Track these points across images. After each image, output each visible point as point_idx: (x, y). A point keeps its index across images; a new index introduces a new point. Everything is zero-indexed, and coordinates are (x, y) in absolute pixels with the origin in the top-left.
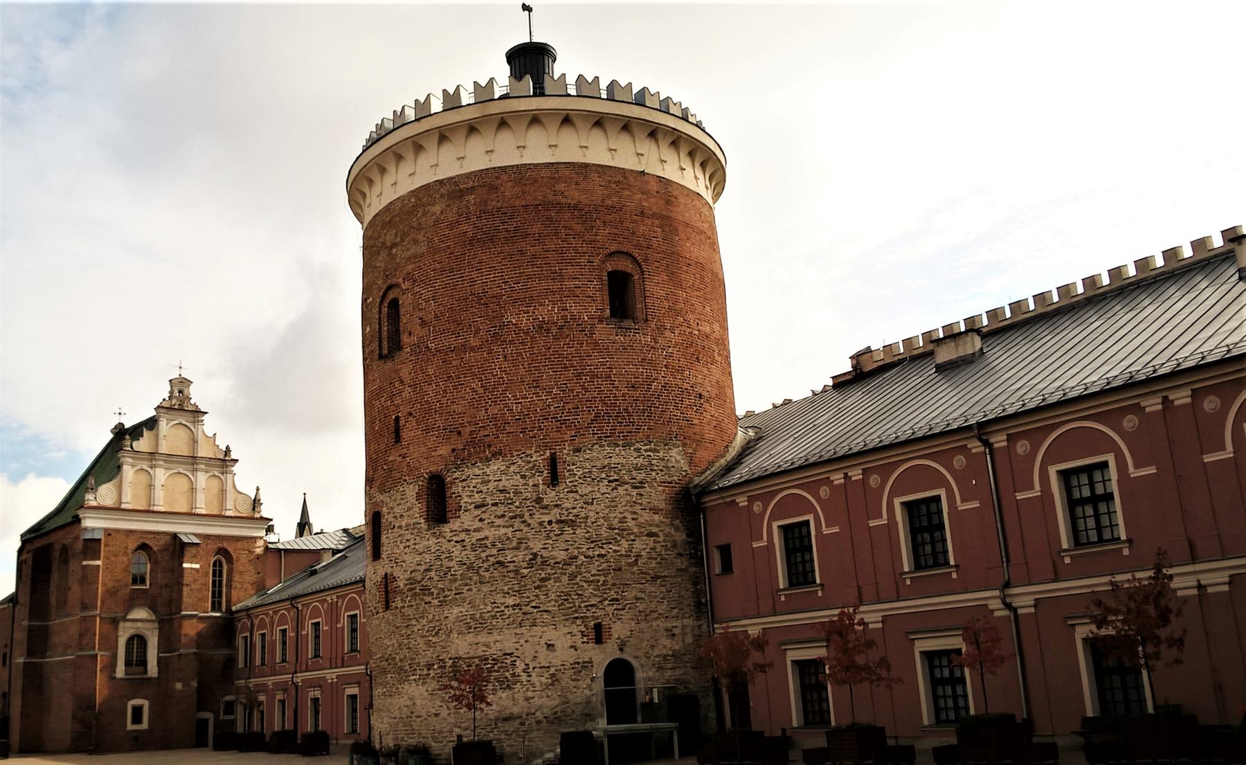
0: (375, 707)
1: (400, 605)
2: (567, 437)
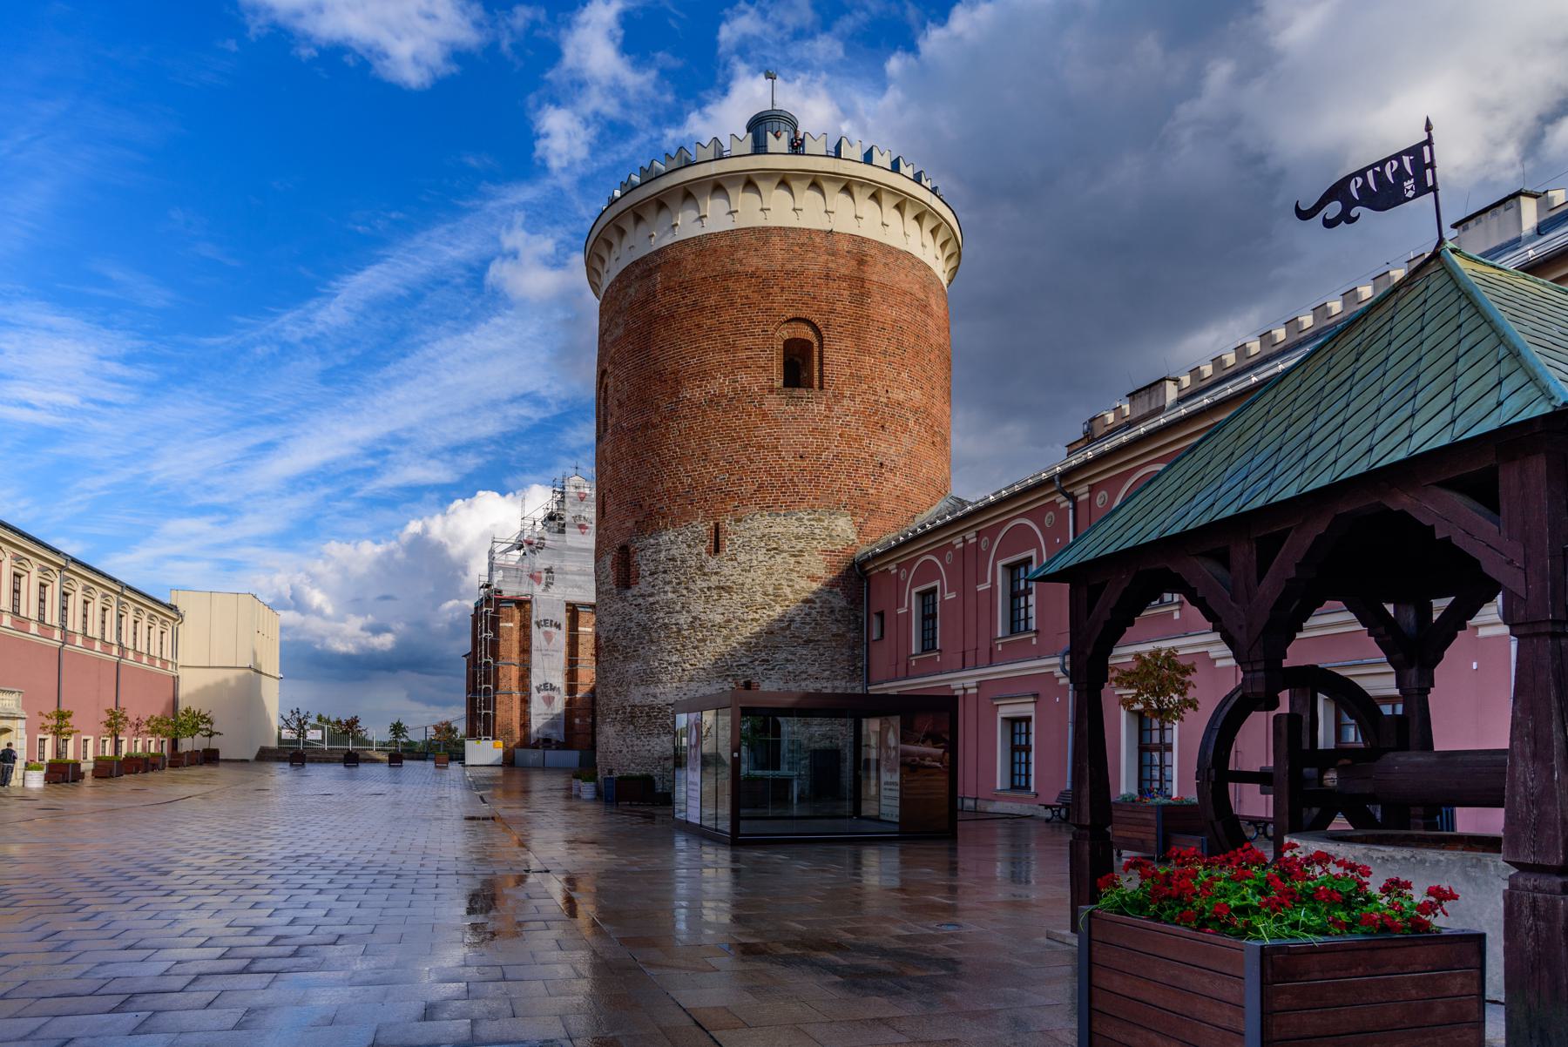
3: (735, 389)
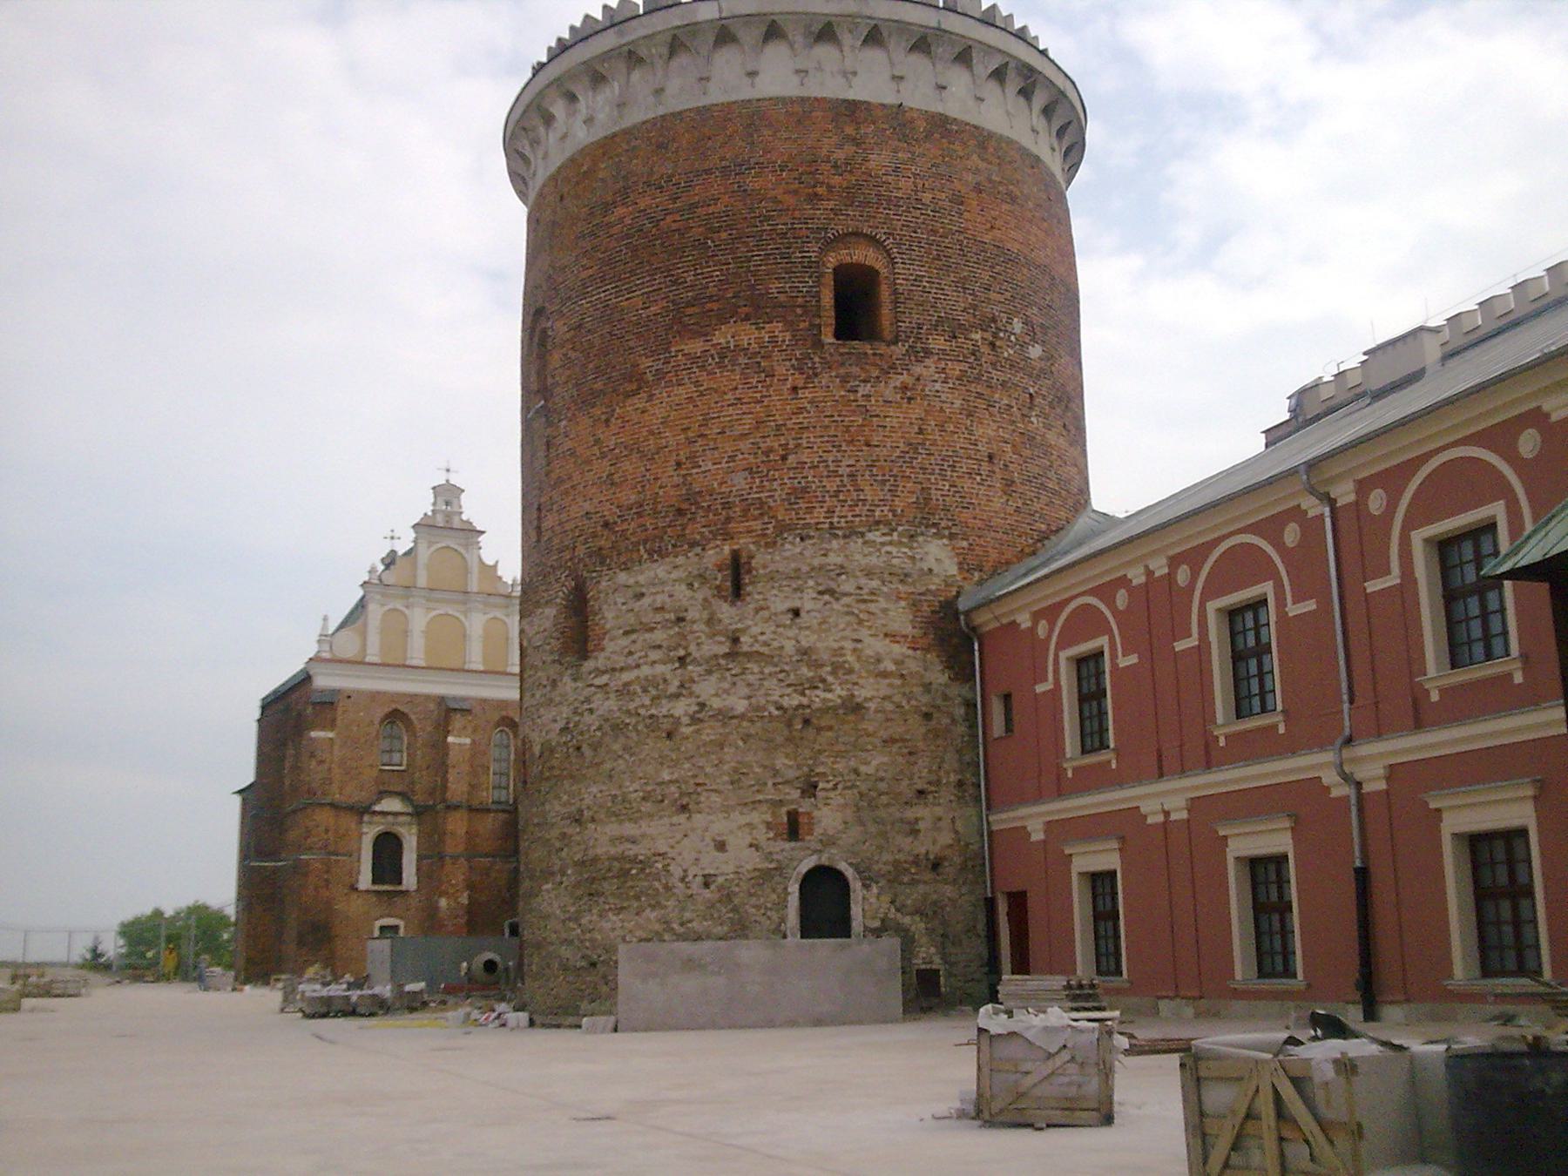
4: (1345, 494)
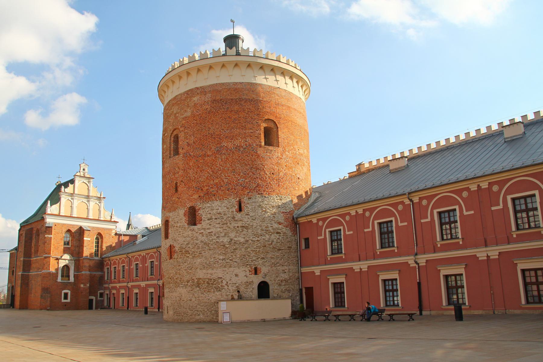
0: (165, 296)
1: (176, 257)
2: (246, 193)
3: (246, 145)
4: (416, 200)
